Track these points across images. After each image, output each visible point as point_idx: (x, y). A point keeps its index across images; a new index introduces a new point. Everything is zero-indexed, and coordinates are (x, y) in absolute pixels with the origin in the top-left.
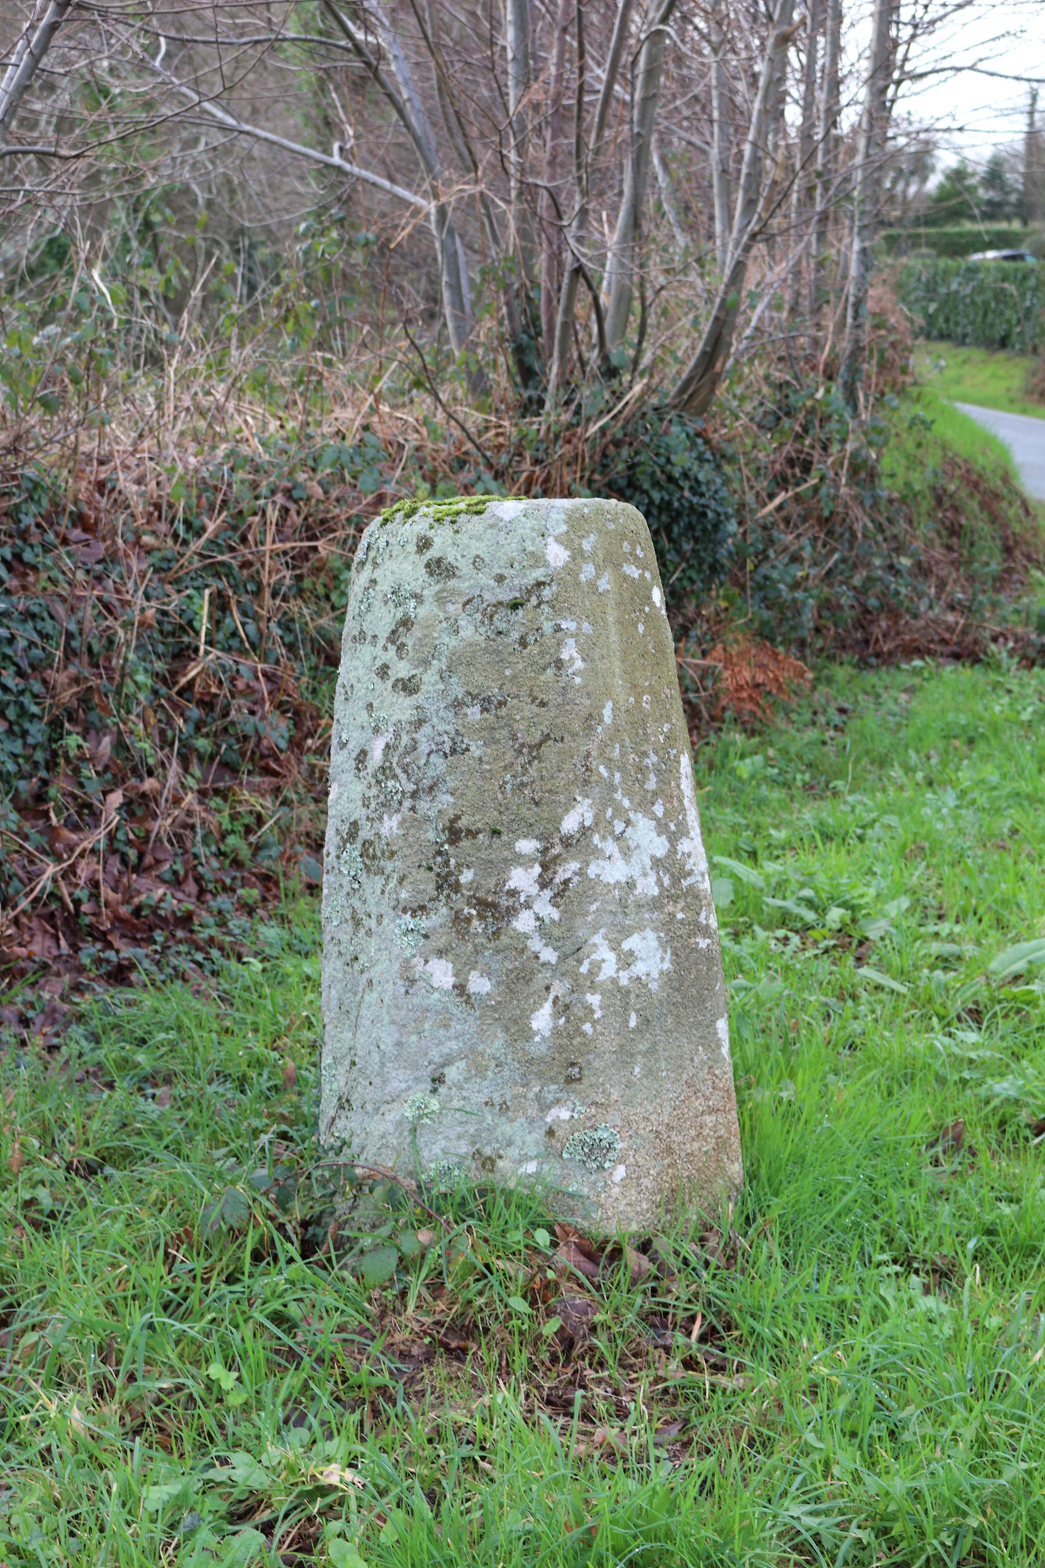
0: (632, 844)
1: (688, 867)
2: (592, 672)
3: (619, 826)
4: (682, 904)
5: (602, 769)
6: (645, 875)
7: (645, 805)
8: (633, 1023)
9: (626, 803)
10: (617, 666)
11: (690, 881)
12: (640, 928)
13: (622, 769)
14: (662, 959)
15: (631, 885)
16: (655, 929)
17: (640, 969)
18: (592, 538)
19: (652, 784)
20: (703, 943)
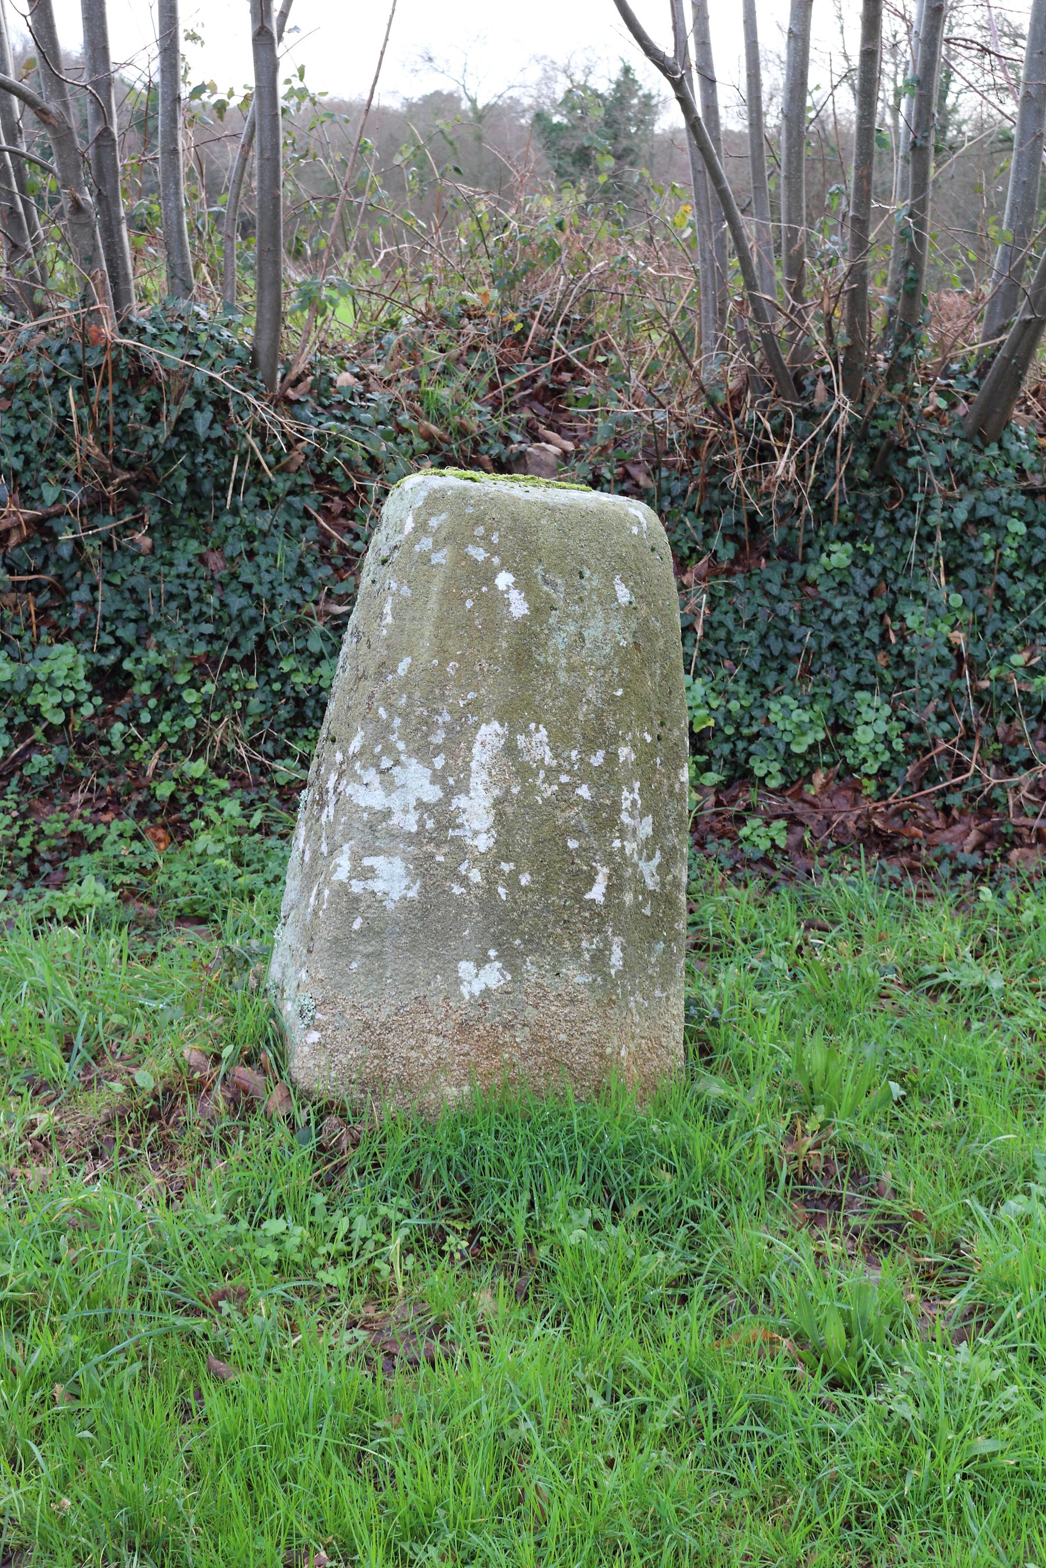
0: (398, 782)
1: (459, 821)
2: (399, 629)
3: (386, 763)
4: (445, 849)
5: (381, 711)
6: (406, 811)
7: (424, 752)
8: (357, 925)
9: (401, 746)
10: (428, 630)
11: (458, 832)
12: (389, 853)
13: (405, 716)
14: (408, 888)
15: (388, 814)
16: (404, 859)
17: (378, 886)
18: (444, 516)
19: (439, 737)
20: (457, 890)
